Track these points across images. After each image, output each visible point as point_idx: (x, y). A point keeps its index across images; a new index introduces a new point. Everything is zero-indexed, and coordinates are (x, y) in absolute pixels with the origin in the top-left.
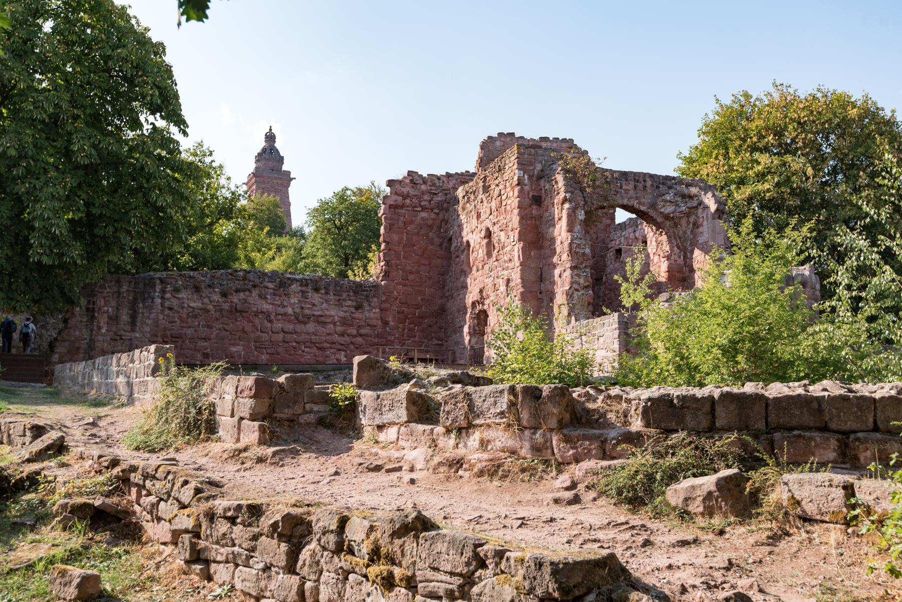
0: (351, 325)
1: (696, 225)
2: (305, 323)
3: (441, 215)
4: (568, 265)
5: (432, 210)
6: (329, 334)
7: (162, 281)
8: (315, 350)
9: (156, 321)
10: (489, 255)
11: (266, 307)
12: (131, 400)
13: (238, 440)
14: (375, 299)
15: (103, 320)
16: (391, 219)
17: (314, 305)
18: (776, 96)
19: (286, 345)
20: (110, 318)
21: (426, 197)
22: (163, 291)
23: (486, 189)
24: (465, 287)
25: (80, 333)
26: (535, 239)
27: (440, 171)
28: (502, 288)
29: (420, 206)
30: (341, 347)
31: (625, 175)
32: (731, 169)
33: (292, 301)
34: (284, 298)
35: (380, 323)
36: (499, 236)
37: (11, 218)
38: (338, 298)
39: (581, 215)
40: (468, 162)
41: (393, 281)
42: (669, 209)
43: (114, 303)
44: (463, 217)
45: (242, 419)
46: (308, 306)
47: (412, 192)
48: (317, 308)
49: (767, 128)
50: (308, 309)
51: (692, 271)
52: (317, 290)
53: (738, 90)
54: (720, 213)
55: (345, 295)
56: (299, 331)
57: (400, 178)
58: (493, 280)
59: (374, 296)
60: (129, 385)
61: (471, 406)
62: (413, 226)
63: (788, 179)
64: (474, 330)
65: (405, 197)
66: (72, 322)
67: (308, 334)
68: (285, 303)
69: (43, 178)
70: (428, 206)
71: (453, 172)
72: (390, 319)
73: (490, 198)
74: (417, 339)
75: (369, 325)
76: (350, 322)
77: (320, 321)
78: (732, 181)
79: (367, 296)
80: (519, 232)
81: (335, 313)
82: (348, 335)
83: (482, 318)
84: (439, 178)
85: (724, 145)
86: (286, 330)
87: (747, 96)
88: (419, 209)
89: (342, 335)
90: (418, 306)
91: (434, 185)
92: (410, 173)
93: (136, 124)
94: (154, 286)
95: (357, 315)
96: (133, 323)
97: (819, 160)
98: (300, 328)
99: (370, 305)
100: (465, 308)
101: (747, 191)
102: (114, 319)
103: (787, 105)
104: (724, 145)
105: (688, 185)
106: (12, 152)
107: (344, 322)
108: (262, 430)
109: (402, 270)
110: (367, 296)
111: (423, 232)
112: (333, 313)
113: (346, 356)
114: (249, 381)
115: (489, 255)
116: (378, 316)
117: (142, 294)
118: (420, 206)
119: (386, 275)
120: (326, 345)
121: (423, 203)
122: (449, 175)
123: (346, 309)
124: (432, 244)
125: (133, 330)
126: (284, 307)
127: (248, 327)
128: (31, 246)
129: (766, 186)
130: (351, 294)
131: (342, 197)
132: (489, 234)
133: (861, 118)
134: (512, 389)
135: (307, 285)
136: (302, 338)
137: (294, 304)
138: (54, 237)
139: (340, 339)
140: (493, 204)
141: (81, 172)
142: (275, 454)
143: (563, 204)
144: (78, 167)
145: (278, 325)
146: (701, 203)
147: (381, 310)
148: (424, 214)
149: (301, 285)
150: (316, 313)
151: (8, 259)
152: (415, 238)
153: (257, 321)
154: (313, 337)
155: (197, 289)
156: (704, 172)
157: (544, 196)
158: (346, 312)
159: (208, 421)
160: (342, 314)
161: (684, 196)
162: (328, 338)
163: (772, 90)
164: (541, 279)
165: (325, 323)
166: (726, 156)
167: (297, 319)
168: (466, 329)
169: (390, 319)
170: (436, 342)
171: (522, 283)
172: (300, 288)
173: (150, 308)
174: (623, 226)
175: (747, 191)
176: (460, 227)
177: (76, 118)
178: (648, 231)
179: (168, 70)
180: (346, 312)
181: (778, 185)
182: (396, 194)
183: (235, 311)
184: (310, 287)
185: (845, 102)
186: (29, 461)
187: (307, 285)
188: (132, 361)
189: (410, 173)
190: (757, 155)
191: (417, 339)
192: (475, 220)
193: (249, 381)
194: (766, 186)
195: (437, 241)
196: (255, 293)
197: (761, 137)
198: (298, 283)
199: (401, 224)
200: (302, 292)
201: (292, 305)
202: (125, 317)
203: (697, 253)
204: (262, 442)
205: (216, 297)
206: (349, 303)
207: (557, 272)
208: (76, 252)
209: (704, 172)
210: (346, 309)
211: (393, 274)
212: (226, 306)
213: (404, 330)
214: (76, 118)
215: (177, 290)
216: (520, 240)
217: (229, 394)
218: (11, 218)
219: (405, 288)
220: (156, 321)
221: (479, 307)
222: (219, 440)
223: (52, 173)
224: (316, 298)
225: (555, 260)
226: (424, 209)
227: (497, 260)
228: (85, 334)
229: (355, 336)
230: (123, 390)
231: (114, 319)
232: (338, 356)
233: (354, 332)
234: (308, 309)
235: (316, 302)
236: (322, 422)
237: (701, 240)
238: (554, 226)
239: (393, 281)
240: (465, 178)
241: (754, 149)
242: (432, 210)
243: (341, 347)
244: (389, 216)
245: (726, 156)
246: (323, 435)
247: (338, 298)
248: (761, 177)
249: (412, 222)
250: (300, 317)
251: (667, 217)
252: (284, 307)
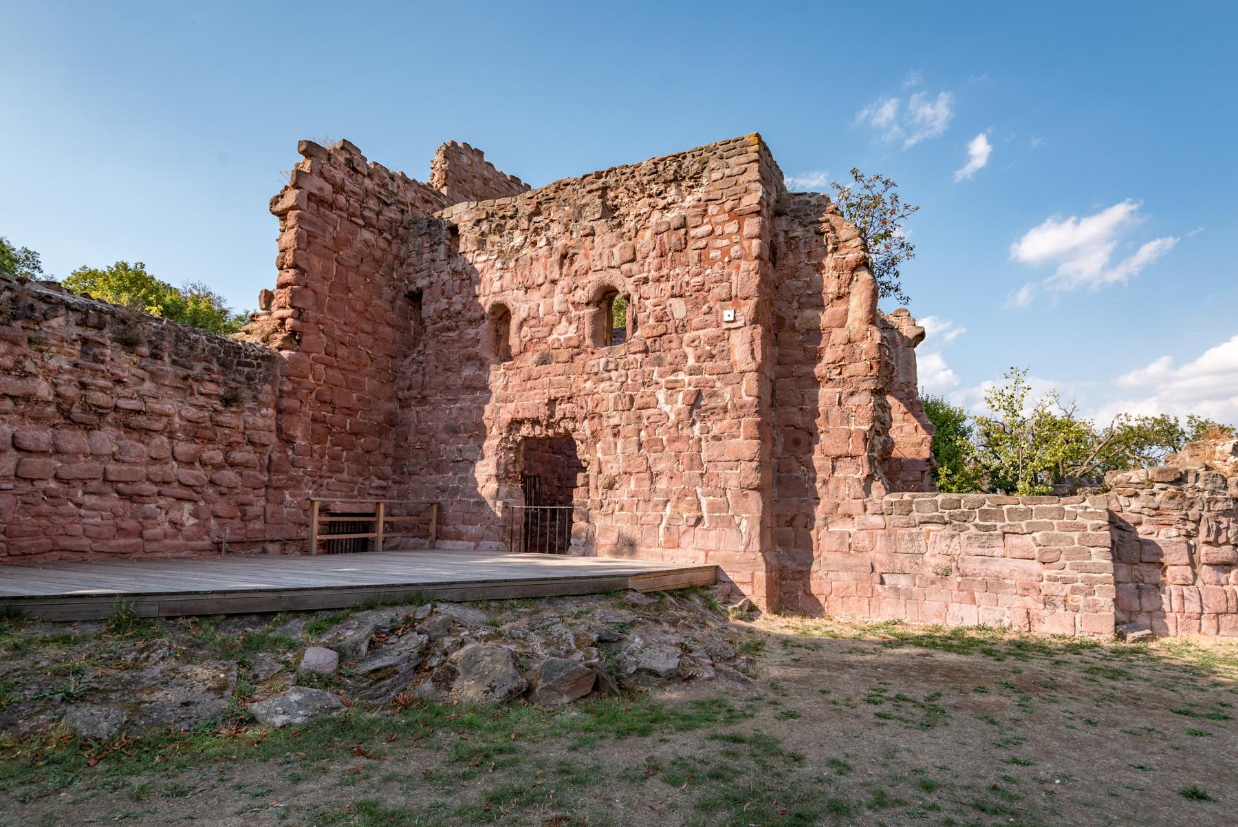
0: (211, 441)
2: (89, 428)
3: (394, 247)
4: (870, 384)
5: (381, 232)
6: (154, 460)
8: (113, 501)
14: (268, 387)
16: (311, 223)
17: (119, 381)
19: (27, 487)
21: (372, 203)
27: (394, 168)
29: (363, 217)
30: (185, 493)
33: (53, 363)
34: (26, 349)
35: (274, 439)
38: (182, 372)
41: (308, 353)
46: (102, 382)
47: (349, 185)
48: (128, 392)
50: (102, 389)
52: (129, 344)
55: (198, 368)
56: (71, 447)
57: (328, 146)
59: (265, 380)
62: (349, 252)
64: (507, 471)
65: (339, 189)
67: (96, 456)
68: (29, 366)
70: (374, 222)
71: (410, 177)
72: (299, 433)
74: (345, 476)
75: (251, 443)
76: (209, 434)
77: (132, 424)
79: (250, 378)
80: (757, 306)
82: (203, 464)
84: (392, 177)
86: (28, 443)
88: (361, 222)
89: (190, 464)
90: (350, 411)
91: (384, 186)
92: (346, 146)
95: (227, 418)
98: (72, 439)
99: (255, 398)
100: (479, 432)
107: (195, 432)
109: (330, 336)
110: (250, 378)
111: (365, 268)
112: (168, 406)
113: (195, 514)
116: (272, 423)
118: (363, 217)
119: (294, 338)
120: (147, 488)
121: (367, 213)
123: (202, 400)
124: (380, 298)
126: (25, 375)
130: (215, 367)
135: (100, 327)
136: (80, 467)
137: (60, 370)
139: (186, 474)
143: (854, 270)
147: (280, 411)
148: (366, 235)
149: (82, 323)
150: (123, 404)
152: (352, 276)
154: (112, 467)
157: (783, 248)
158: (201, 408)
160: (192, 413)
162: (153, 469)
165: (148, 431)
167: (66, 414)
169: (299, 433)
170: (377, 482)
171: (759, 404)
172: (79, 330)
180: (201, 408)
182: (321, 175)
184: (107, 333)
187: (100, 327)
189: (346, 146)
191: (345, 476)
198: (73, 317)
199: (329, 241)
200: (85, 341)
201: (52, 375)
206: (210, 388)
207: (826, 394)
210: (202, 400)
211: (309, 339)
213: (322, 457)
216: (755, 321)
219: (330, 372)
224: (124, 364)
225: (819, 370)
226: (368, 225)
227: (646, 351)
229: (218, 467)
232: (174, 515)
233: (219, 457)
234: (102, 389)
235: (125, 375)
238: (821, 306)
239: (308, 353)
242: (381, 232)
243: (185, 493)
244: (307, 215)
247: (182, 372)
249: (348, 243)
250: (76, 411)
252: (25, 375)
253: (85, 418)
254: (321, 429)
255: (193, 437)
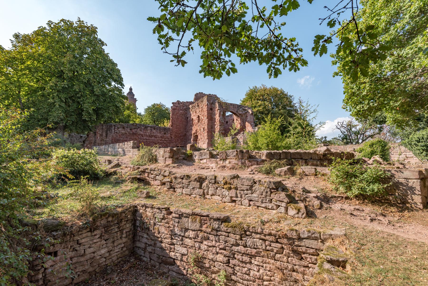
1: (247, 117)
7: (114, 126)
9: (113, 136)
10: (199, 122)
11: (142, 133)
12: (124, 154)
13: (165, 163)
15: (98, 135)
18: (262, 88)
20: (100, 135)
22: (115, 128)
23: (198, 106)
24: (192, 129)
25: (92, 138)
26: (211, 119)
28: (202, 130)
31: (231, 104)
32: (253, 104)
36: (201, 117)
37: (76, 108)
39: (222, 113)
40: (192, 99)
42: (241, 113)
43: (101, 131)
44: (191, 112)
45: (166, 158)
49: (261, 95)
51: (245, 127)
52: (155, 129)
53: (254, 86)
54: (252, 114)
58: (200, 128)
60: (124, 151)
61: (227, 154)
63: (265, 107)
66: (90, 136)
69: (86, 98)
73: (199, 108)
77: (155, 137)
78: (253, 107)
81: (159, 135)
83: (196, 137)
85: (251, 98)
87: (256, 87)
93: (110, 84)
94: (112, 127)
95: (165, 135)
96: (106, 136)
97: (271, 103)
98: (150, 138)
101: (256, 109)
102: (101, 135)
103: (265, 90)
104: (251, 98)
105: (245, 107)
106: (77, 90)
107: (161, 137)
108: (173, 160)
114: (168, 149)
115: (199, 122)
117: (109, 128)
119: (172, 126)
122: (187, 102)
125: (107, 138)
127: (137, 138)
128: (83, 115)
129: (261, 108)
131: (154, 106)
132: (199, 117)
133: (280, 93)
134: (237, 151)
136: (151, 141)
138: (89, 113)
139: (160, 141)
140: (200, 110)
141: (96, 96)
142: (177, 166)
144: (95, 95)
145: (145, 138)
146: (248, 111)
151: (76, 118)
153: (139, 137)
155: (124, 128)
156: (247, 104)
159: (155, 159)
161: (244, 110)
163: (261, 86)
164: (212, 128)
166: (252, 101)
168: (192, 140)
173: (111, 133)
174: (228, 116)
175: (256, 109)
176: (191, 115)
177: (95, 82)
178: (235, 117)
179: (119, 71)
181: (263, 108)
183: (134, 134)
185: (276, 90)
186: (111, 168)
188: (124, 145)
190: (258, 101)
192: (195, 113)
193: (168, 149)
194: (261, 108)
195: (184, 118)
196: (139, 129)
197: (259, 97)
202: (104, 135)
203: (247, 123)
204: (172, 163)
205: (129, 130)
208: (95, 117)
209: (247, 104)
212: (131, 133)
214: (95, 82)
215: (118, 128)
217: (161, 153)
218: (76, 108)
220: (113, 136)
221: (195, 134)
222: (159, 163)
223: (88, 96)
224: (154, 131)
228: (94, 139)
230: (122, 152)
231: (101, 135)
233: (164, 140)
236: (184, 159)
237: (248, 120)
240: (191, 103)
241: (258, 100)
245: (252, 101)
246: (185, 162)
248: (260, 106)
251: (240, 114)
253: (151, 136)
254: (176, 136)
255: (161, 138)
